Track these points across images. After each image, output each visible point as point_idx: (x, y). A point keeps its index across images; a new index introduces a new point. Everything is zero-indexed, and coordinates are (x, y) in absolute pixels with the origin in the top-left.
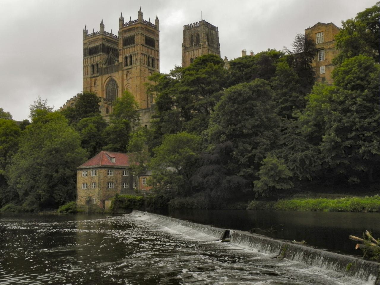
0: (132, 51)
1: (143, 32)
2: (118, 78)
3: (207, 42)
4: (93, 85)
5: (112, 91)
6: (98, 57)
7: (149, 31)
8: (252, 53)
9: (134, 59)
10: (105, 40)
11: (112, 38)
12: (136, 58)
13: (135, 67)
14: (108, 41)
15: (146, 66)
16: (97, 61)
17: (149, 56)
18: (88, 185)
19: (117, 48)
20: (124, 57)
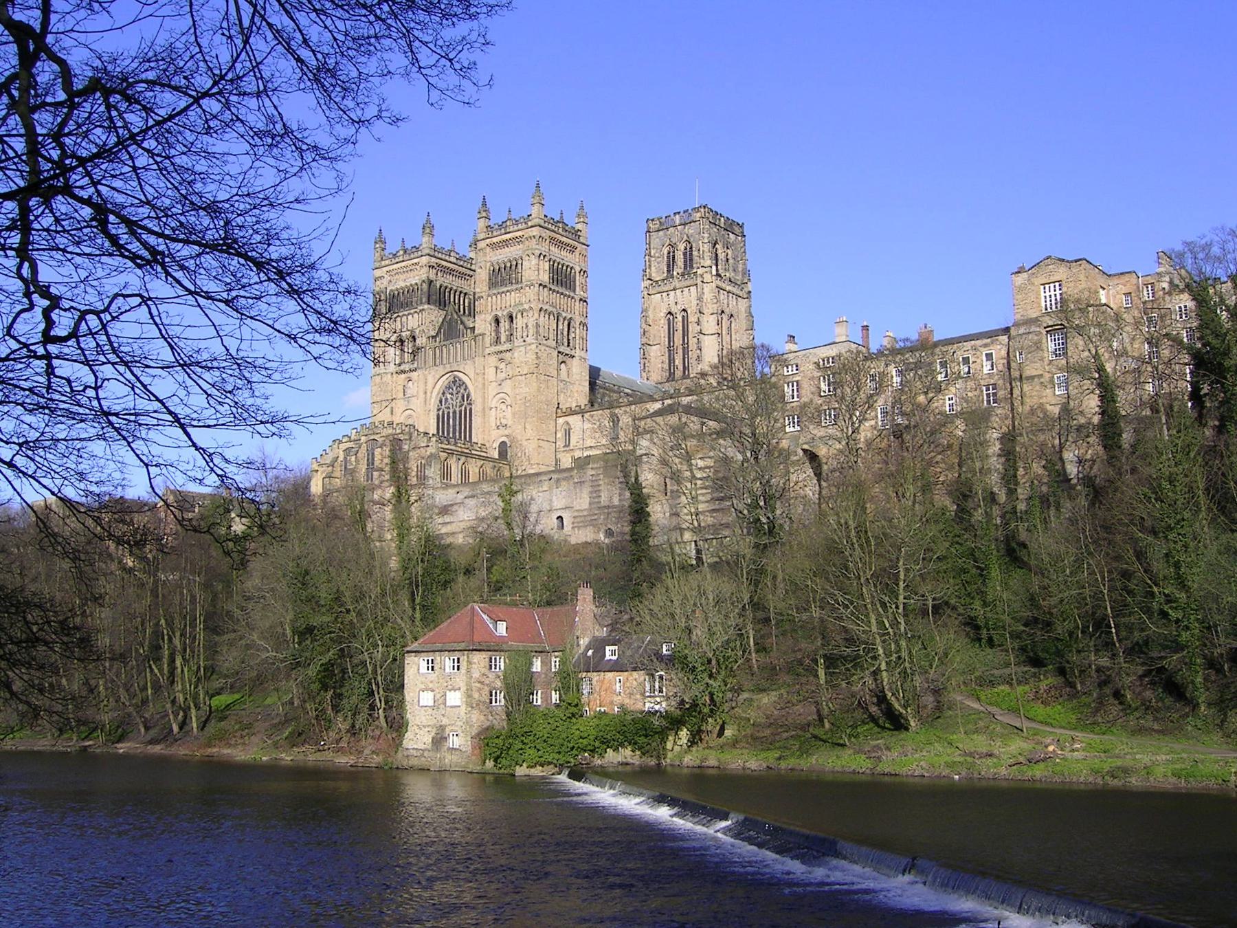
1: (544, 247)
5: (455, 412)
9: (519, 326)
12: (525, 321)
13: (522, 349)
20: (490, 318)
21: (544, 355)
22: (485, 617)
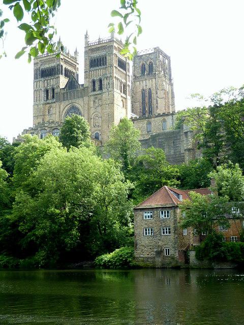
0: (102, 74)
4: (47, 113)
6: (54, 80)
15: (119, 92)
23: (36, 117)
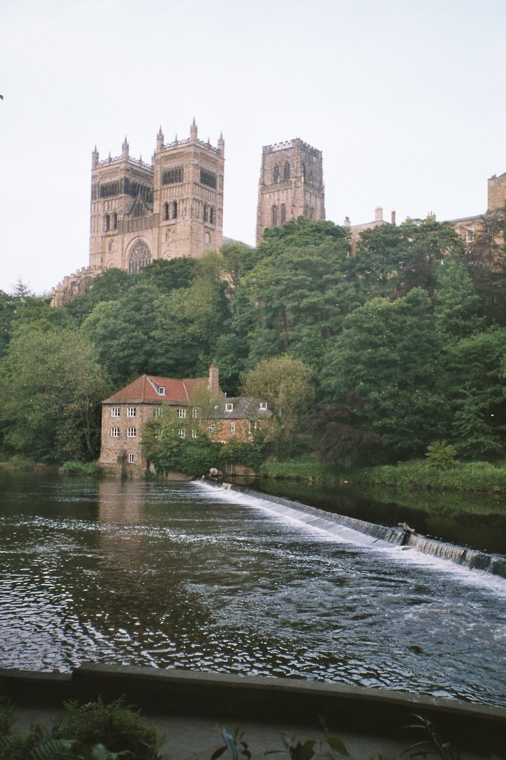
2: (151, 239)
3: (303, 178)
4: (107, 250)
5: (140, 262)
6: (117, 201)
7: (207, 159)
8: (394, 213)
9: (181, 209)
10: (130, 172)
11: (142, 169)
12: (184, 206)
14: (136, 173)
15: (201, 220)
16: (115, 209)
17: (206, 202)
18: (122, 431)
19: (149, 185)
20: (163, 203)
21: (195, 228)
22: (152, 384)
23: (92, 255)
